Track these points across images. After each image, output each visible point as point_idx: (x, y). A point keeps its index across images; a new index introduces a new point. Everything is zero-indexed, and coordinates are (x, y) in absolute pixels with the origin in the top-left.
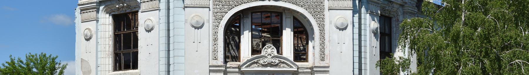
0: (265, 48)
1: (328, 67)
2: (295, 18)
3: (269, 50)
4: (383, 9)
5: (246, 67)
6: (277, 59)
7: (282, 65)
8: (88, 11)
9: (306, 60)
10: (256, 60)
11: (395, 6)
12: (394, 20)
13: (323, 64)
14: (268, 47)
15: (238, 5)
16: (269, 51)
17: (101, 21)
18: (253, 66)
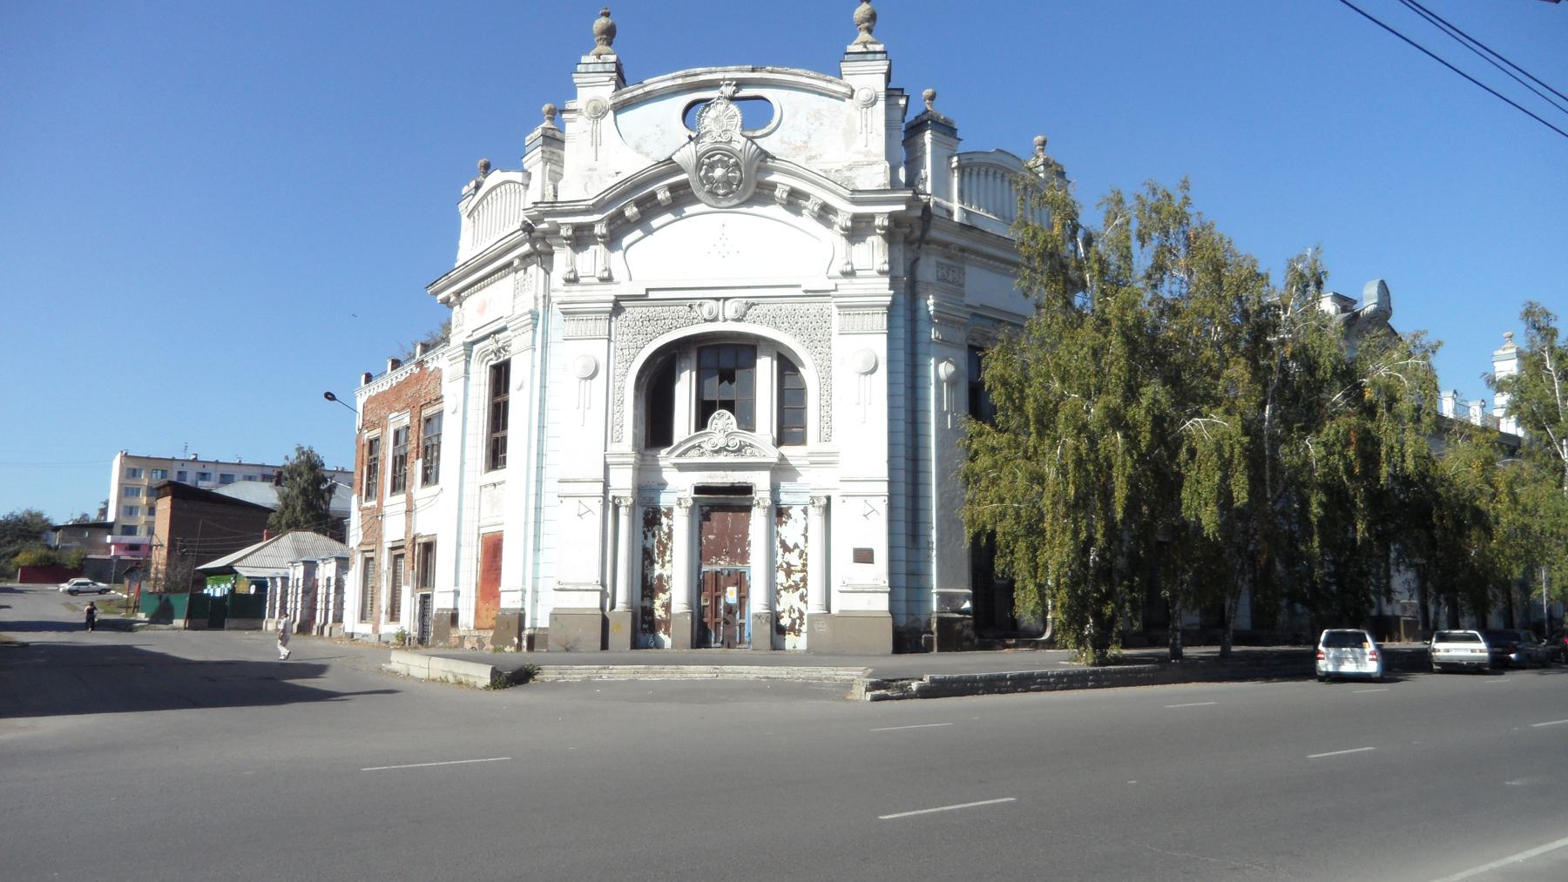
0: (715, 418)
1: (835, 454)
3: (723, 421)
5: (678, 456)
9: (801, 440)
10: (696, 442)
13: (826, 447)
14: (719, 414)
15: (663, 333)
18: (691, 453)
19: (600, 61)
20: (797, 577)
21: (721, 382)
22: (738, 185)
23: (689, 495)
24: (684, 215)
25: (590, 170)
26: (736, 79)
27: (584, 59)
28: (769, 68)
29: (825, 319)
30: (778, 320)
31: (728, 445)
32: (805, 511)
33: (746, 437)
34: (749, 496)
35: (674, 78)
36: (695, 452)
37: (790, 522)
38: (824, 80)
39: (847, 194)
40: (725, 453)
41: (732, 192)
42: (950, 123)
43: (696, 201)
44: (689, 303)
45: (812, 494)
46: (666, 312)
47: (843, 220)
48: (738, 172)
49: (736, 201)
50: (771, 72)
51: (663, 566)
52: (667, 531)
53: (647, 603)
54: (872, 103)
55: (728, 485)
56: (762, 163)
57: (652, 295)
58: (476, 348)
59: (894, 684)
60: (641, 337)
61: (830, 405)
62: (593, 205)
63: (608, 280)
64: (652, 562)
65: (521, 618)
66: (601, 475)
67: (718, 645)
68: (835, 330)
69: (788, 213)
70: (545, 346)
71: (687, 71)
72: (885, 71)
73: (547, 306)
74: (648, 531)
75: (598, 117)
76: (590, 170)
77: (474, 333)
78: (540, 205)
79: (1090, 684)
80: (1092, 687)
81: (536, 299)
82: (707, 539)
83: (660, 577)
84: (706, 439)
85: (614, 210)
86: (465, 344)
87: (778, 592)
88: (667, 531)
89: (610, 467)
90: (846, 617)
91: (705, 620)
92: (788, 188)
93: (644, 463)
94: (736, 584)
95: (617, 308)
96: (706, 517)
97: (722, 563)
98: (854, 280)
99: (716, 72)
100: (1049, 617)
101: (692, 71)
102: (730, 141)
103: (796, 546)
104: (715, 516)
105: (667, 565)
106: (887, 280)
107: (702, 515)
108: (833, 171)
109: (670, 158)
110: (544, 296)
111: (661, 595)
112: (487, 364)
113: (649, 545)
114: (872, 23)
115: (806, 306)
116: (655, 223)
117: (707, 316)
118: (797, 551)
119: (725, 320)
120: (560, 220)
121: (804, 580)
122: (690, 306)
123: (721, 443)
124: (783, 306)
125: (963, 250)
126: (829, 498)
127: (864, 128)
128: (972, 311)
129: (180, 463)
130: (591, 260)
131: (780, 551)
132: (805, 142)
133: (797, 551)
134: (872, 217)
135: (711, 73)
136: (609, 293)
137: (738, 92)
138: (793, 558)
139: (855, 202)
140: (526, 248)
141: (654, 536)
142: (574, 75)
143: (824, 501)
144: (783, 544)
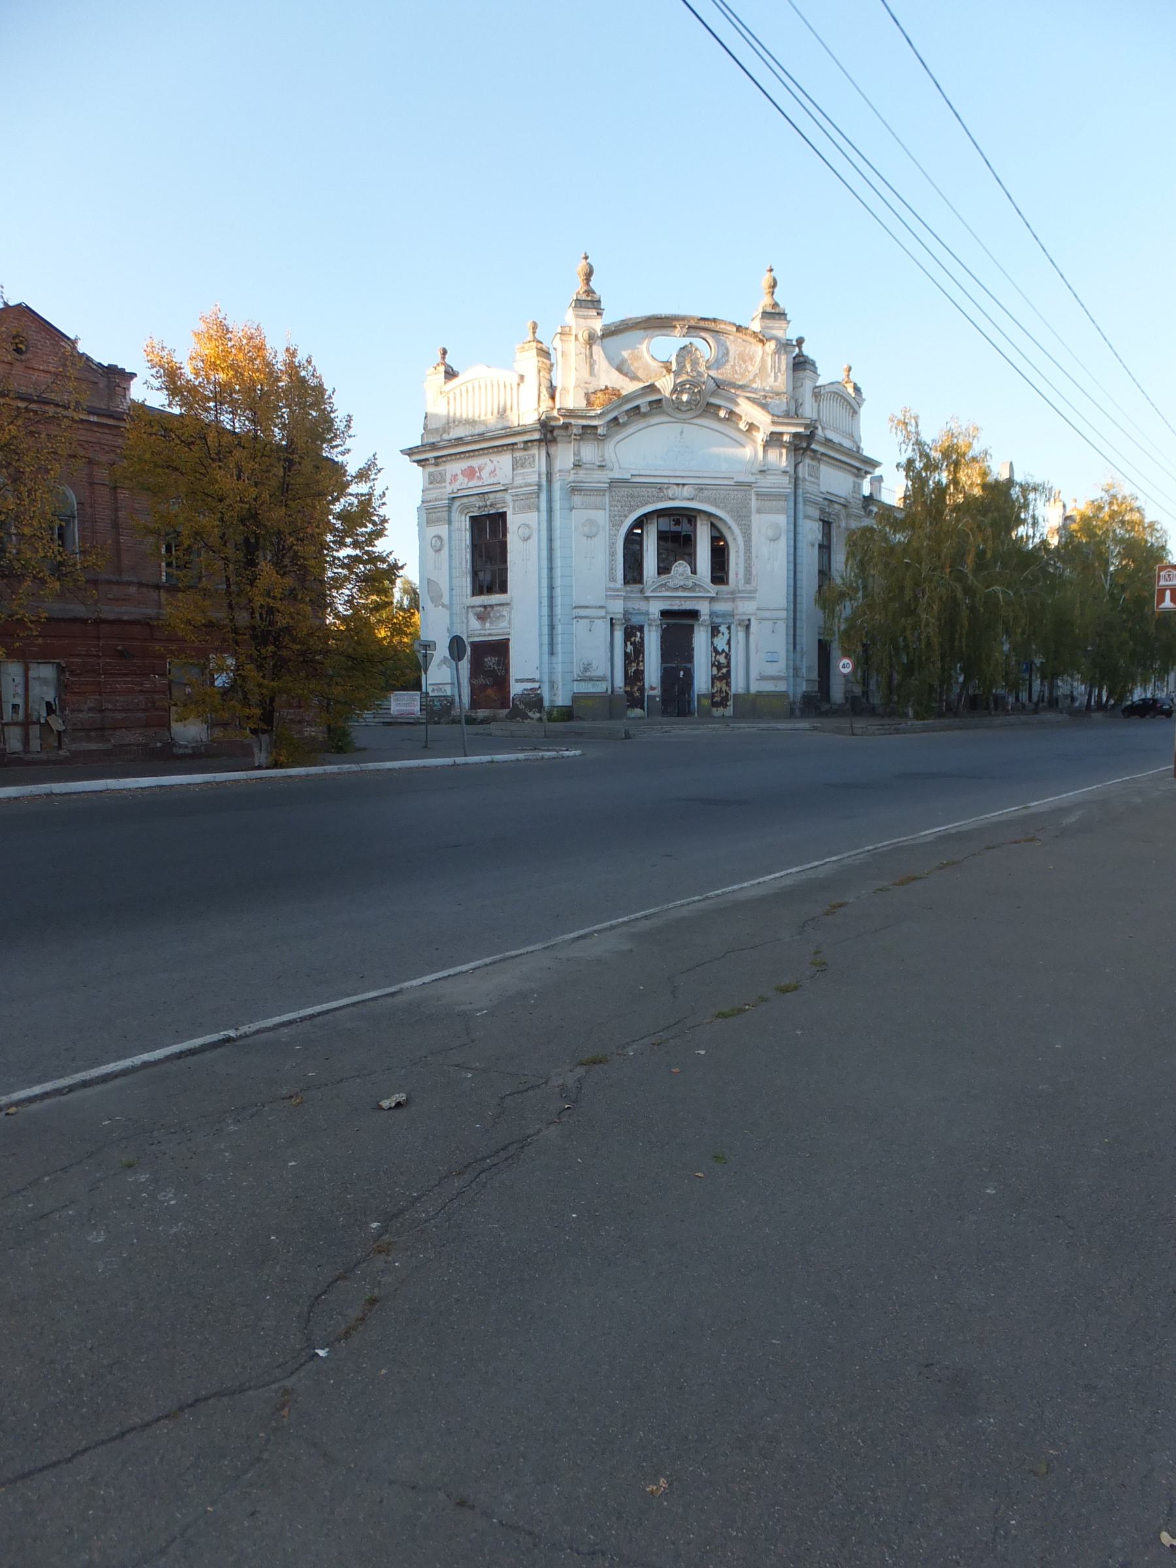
2: (712, 525)
3: (680, 568)
4: (822, 511)
5: (652, 591)
6: (691, 581)
7: (697, 589)
8: (436, 510)
11: (836, 506)
12: (834, 526)
13: (748, 587)
16: (681, 569)
17: (455, 525)
19: (589, 298)
20: (724, 670)
23: (657, 615)
25: (586, 383)
29: (746, 504)
32: (729, 628)
37: (720, 635)
44: (659, 486)
46: (643, 492)
51: (638, 664)
57: (634, 480)
58: (457, 503)
60: (627, 509)
65: (541, 700)
68: (754, 509)
70: (550, 510)
73: (550, 481)
76: (586, 383)
77: (460, 492)
81: (539, 475)
84: (670, 580)
86: (449, 499)
90: (759, 694)
98: (768, 477)
103: (723, 651)
105: (641, 664)
110: (547, 474)
112: (466, 514)
115: (736, 493)
117: (671, 496)
118: (724, 655)
120: (572, 421)
121: (729, 672)
123: (682, 583)
125: (823, 454)
126: (749, 620)
128: (823, 496)
130: (589, 452)
133: (724, 655)
134: (781, 434)
136: (604, 476)
138: (722, 659)
140: (536, 436)
144: (715, 650)
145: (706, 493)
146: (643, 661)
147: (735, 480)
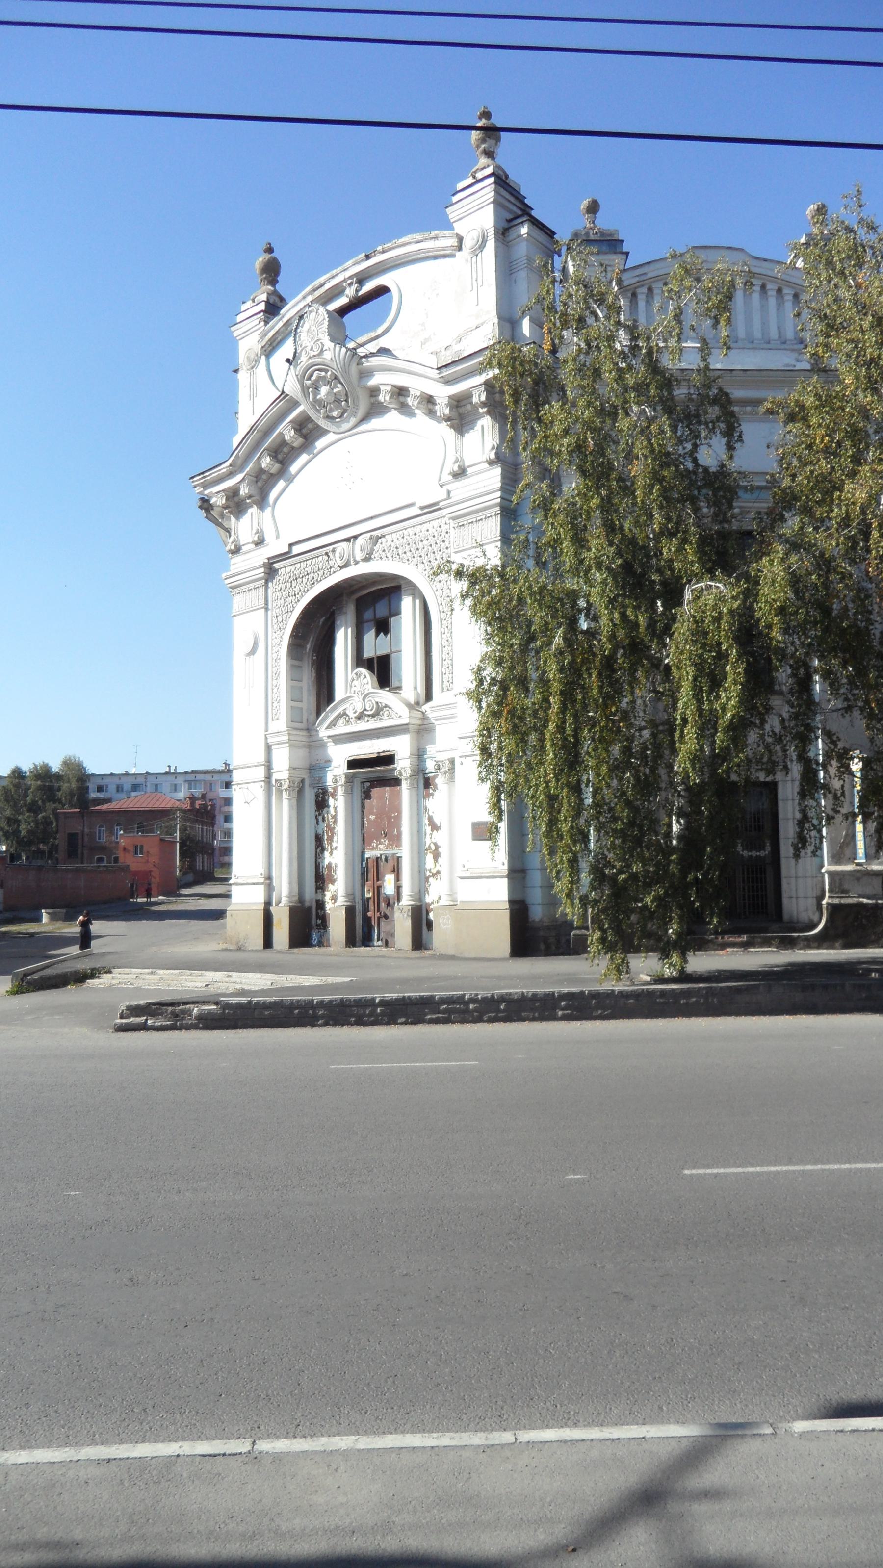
21: (377, 635)
22: (347, 401)
24: (315, 451)
26: (356, 275)
27: (244, 307)
28: (380, 248)
30: (400, 551)
31: (365, 710)
33: (385, 696)
34: (392, 766)
35: (304, 298)
36: (341, 721)
38: (431, 238)
39: (435, 374)
40: (367, 718)
41: (345, 411)
42: (611, 235)
43: (324, 432)
45: (437, 759)
47: (443, 409)
48: (339, 385)
49: (353, 421)
50: (383, 252)
51: (331, 854)
52: (334, 814)
53: (319, 897)
54: (480, 247)
55: (375, 755)
56: (360, 366)
57: (296, 550)
59: (170, 1009)
61: (451, 645)
62: (231, 465)
63: (260, 542)
64: (323, 850)
66: (262, 758)
67: (380, 943)
69: (403, 417)
71: (313, 284)
72: (492, 199)
74: (320, 814)
75: (252, 368)
78: (195, 479)
79: (560, 1013)
80: (566, 1018)
82: (369, 820)
83: (330, 865)
85: (251, 465)
87: (427, 879)
88: (334, 814)
89: (273, 747)
91: (369, 914)
92: (389, 388)
93: (311, 739)
94: (394, 871)
95: (270, 571)
96: (367, 795)
97: (381, 846)
99: (337, 275)
100: (824, 902)
101: (317, 283)
102: (322, 351)
104: (375, 792)
105: (334, 852)
106: (497, 471)
107: (364, 792)
108: (443, 349)
109: (283, 392)
111: (330, 886)
113: (320, 832)
114: (493, 142)
115: (426, 526)
116: (294, 468)
117: (340, 563)
119: (357, 563)
122: (327, 554)
124: (405, 532)
126: (452, 762)
127: (474, 282)
129: (154, 777)
131: (429, 829)
132: (423, 324)
135: (333, 277)
136: (261, 556)
137: (360, 290)
139: (448, 382)
141: (323, 820)
142: (233, 329)
143: (447, 765)
145: (384, 543)
146: (336, 848)
147: (418, 505)
